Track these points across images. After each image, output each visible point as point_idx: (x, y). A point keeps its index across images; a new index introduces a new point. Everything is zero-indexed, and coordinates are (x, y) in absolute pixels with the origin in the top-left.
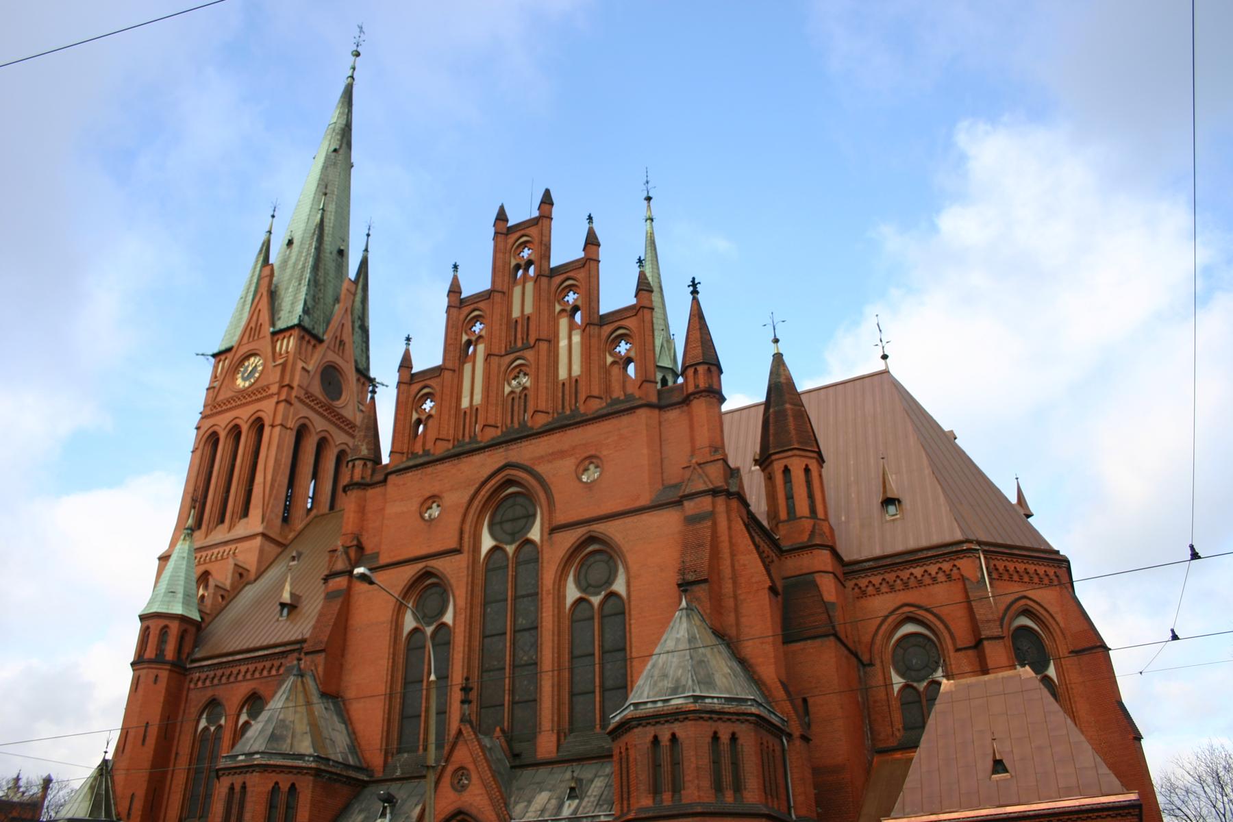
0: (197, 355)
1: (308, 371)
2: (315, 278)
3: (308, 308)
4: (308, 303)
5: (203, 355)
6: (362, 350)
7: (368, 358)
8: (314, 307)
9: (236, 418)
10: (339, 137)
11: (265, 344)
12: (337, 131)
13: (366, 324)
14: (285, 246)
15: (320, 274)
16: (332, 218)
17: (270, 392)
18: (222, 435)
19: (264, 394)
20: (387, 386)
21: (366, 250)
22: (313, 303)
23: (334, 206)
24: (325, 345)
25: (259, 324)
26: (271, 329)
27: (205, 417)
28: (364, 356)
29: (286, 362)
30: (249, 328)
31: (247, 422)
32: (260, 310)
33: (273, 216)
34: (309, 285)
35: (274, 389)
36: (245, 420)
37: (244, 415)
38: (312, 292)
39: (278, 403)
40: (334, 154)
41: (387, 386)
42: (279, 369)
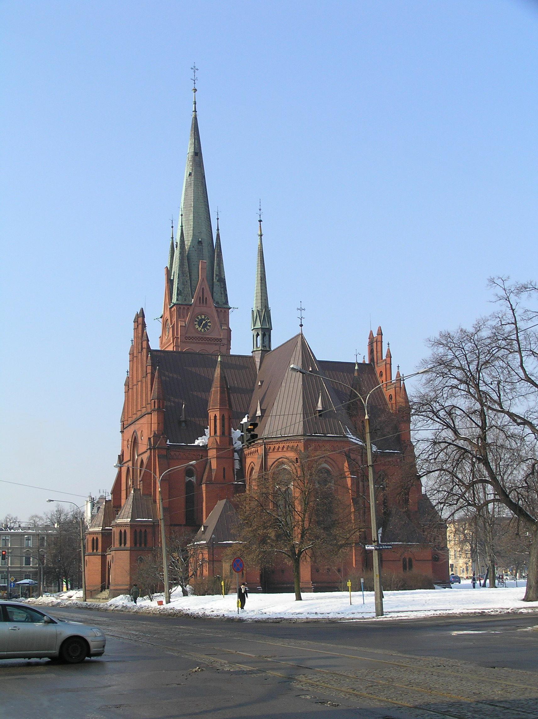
3: (181, 291)
4: (180, 288)
6: (221, 293)
7: (226, 295)
8: (183, 289)
12: (189, 160)
13: (223, 277)
15: (185, 266)
16: (192, 223)
21: (218, 230)
22: (183, 286)
23: (192, 215)
24: (193, 306)
26: (169, 307)
28: (223, 296)
33: (172, 227)
34: (178, 278)
38: (181, 281)
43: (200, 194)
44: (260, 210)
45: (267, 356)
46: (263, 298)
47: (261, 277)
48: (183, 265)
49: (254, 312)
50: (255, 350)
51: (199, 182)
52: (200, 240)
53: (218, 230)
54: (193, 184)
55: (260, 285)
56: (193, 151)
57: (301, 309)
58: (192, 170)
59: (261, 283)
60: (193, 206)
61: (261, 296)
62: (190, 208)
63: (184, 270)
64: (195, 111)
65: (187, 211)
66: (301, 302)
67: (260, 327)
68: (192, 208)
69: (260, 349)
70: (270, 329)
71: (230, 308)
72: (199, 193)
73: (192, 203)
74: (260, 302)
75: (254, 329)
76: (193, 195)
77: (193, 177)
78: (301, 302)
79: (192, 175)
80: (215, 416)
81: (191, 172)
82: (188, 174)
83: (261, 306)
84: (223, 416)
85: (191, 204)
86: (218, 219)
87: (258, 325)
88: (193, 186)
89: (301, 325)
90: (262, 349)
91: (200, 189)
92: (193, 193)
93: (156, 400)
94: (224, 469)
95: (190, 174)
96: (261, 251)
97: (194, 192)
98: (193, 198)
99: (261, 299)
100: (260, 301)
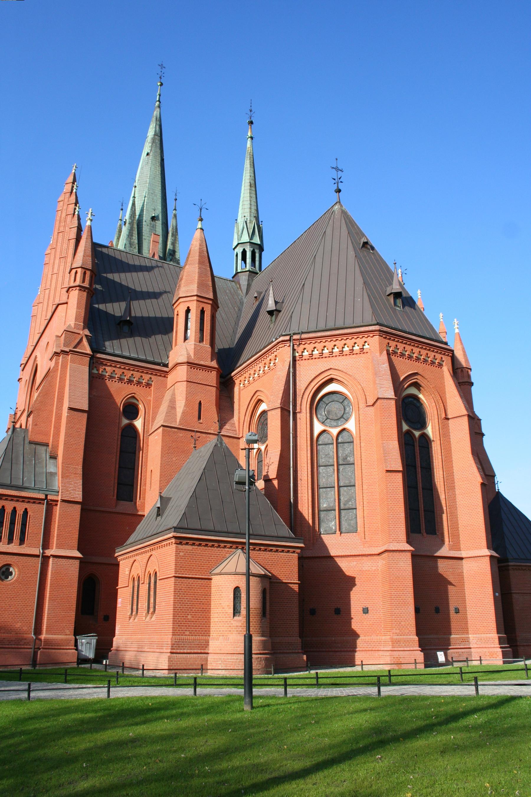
2: (130, 241)
10: (150, 145)
15: (134, 238)
40: (148, 156)
43: (157, 173)
44: (251, 111)
45: (257, 279)
46: (252, 207)
47: (250, 182)
48: (132, 236)
49: (239, 225)
50: (239, 271)
51: (157, 163)
52: (153, 215)
53: (175, 209)
54: (150, 163)
55: (249, 192)
56: (154, 134)
57: (337, 169)
58: (151, 150)
59: (250, 189)
60: (148, 182)
61: (251, 204)
62: (145, 185)
63: (132, 241)
65: (141, 188)
66: (337, 159)
67: (248, 241)
68: (147, 185)
69: (247, 270)
70: (261, 248)
72: (156, 172)
73: (148, 180)
74: (249, 211)
75: (238, 244)
76: (149, 173)
77: (151, 157)
78: (337, 159)
79: (151, 154)
80: (188, 311)
81: (149, 152)
82: (146, 154)
83: (250, 216)
84: (202, 312)
85: (147, 181)
86: (176, 200)
87: (245, 238)
88: (150, 165)
89: (339, 191)
90: (251, 270)
91: (157, 169)
92: (149, 171)
93: (79, 270)
94: (200, 403)
95: (148, 154)
96: (252, 154)
97: (150, 170)
98: (149, 175)
99: (250, 208)
100: (248, 210)
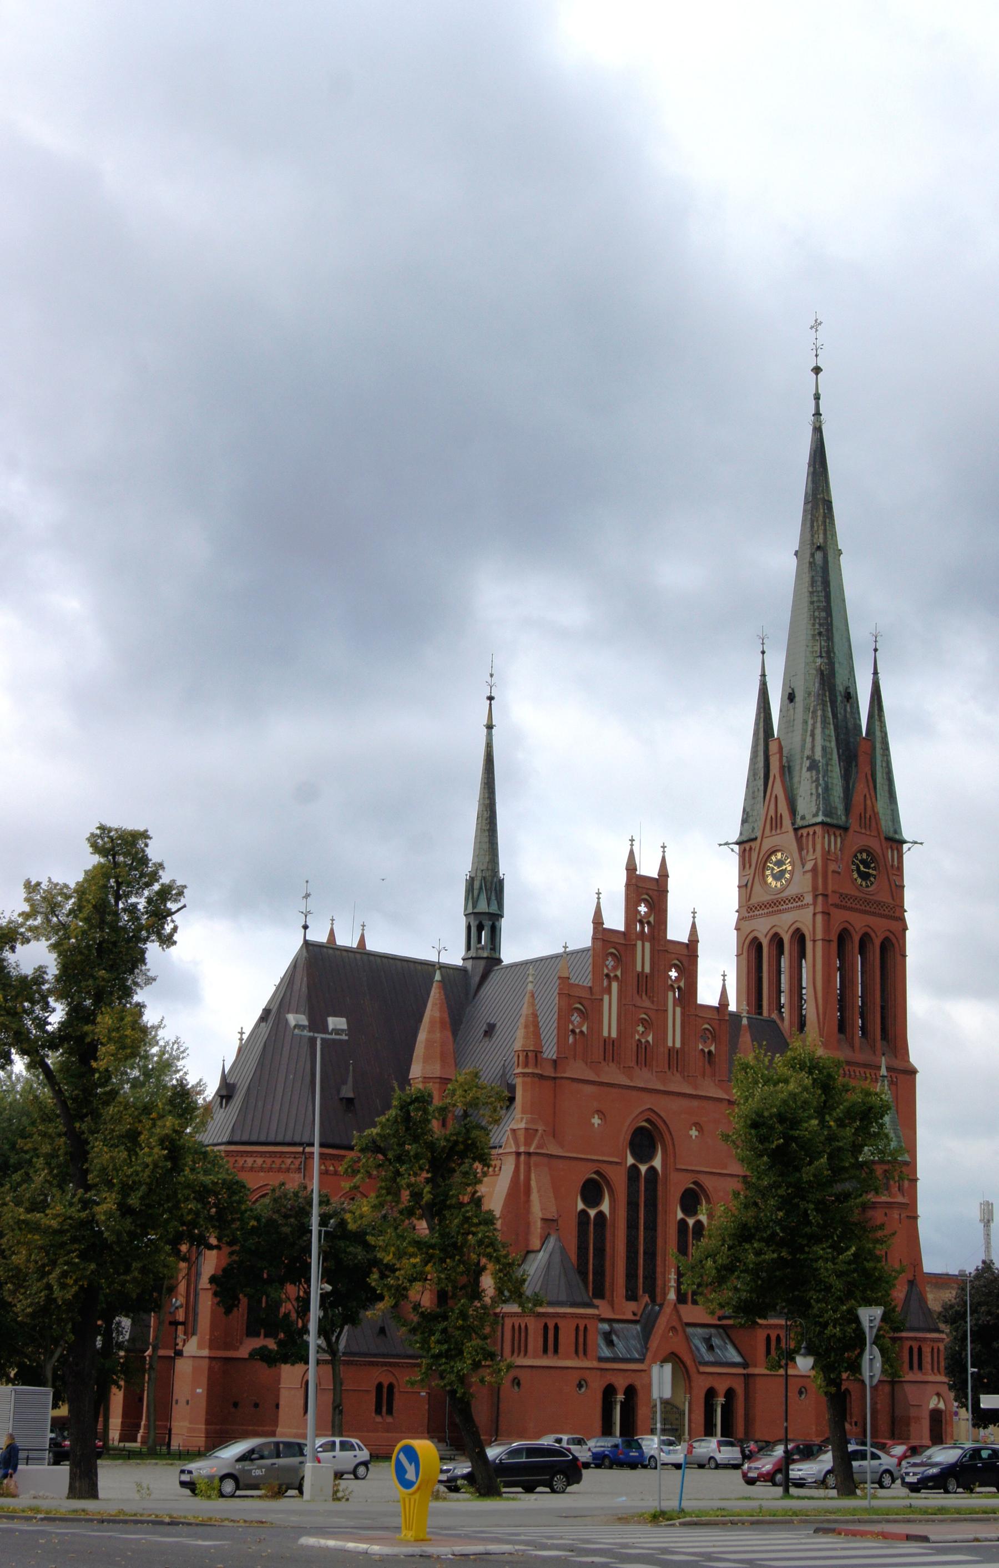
0: (720, 845)
1: (839, 873)
5: (727, 844)
9: (774, 926)
11: (788, 838)
14: (787, 701)
17: (805, 902)
18: (765, 943)
19: (800, 903)
20: (921, 843)
25: (779, 815)
27: (741, 919)
29: (815, 865)
30: (769, 817)
31: (787, 932)
32: (776, 797)
35: (809, 899)
36: (786, 929)
37: (784, 923)
39: (814, 914)
41: (921, 843)
42: (809, 876)
64: (817, 414)
71: (905, 842)
